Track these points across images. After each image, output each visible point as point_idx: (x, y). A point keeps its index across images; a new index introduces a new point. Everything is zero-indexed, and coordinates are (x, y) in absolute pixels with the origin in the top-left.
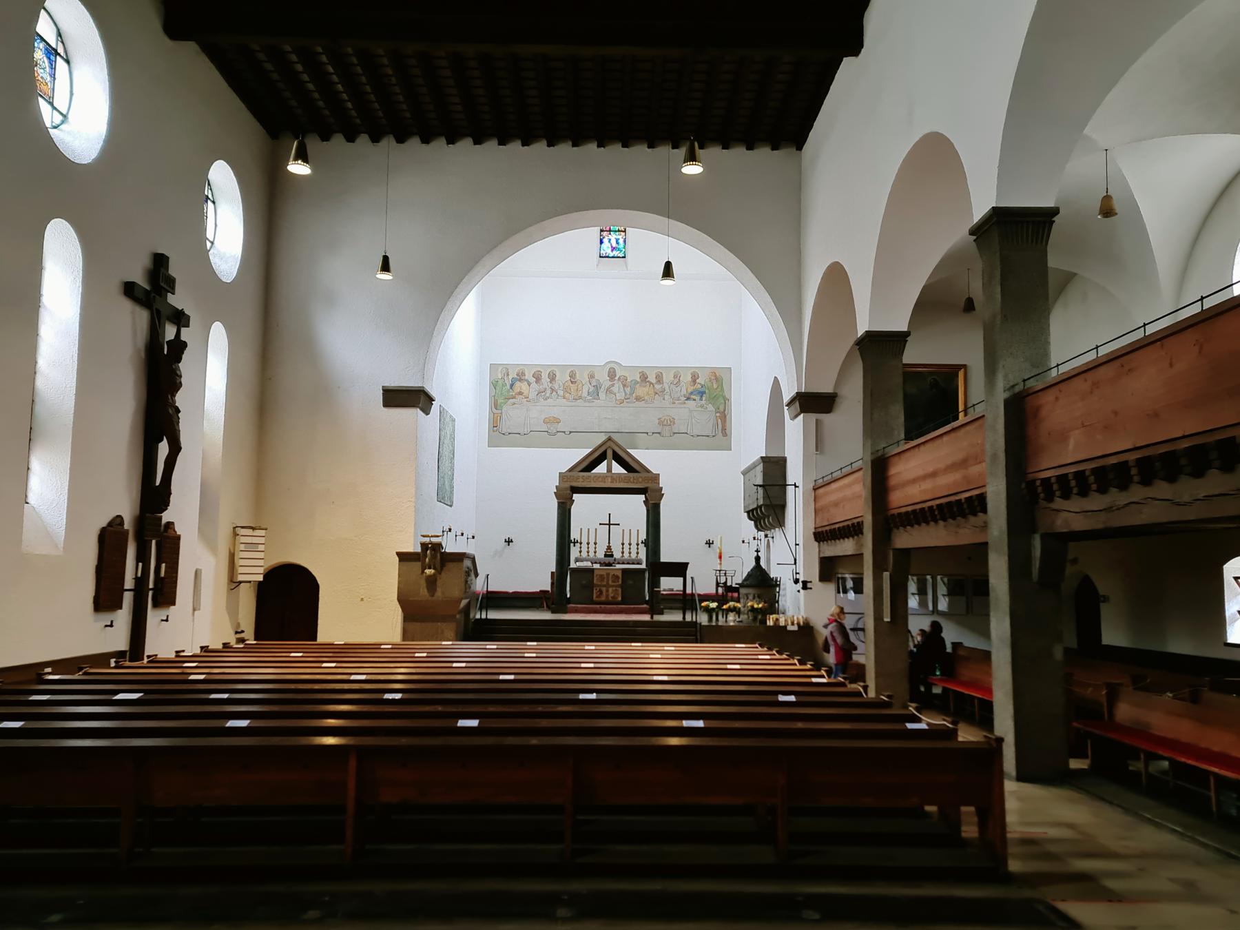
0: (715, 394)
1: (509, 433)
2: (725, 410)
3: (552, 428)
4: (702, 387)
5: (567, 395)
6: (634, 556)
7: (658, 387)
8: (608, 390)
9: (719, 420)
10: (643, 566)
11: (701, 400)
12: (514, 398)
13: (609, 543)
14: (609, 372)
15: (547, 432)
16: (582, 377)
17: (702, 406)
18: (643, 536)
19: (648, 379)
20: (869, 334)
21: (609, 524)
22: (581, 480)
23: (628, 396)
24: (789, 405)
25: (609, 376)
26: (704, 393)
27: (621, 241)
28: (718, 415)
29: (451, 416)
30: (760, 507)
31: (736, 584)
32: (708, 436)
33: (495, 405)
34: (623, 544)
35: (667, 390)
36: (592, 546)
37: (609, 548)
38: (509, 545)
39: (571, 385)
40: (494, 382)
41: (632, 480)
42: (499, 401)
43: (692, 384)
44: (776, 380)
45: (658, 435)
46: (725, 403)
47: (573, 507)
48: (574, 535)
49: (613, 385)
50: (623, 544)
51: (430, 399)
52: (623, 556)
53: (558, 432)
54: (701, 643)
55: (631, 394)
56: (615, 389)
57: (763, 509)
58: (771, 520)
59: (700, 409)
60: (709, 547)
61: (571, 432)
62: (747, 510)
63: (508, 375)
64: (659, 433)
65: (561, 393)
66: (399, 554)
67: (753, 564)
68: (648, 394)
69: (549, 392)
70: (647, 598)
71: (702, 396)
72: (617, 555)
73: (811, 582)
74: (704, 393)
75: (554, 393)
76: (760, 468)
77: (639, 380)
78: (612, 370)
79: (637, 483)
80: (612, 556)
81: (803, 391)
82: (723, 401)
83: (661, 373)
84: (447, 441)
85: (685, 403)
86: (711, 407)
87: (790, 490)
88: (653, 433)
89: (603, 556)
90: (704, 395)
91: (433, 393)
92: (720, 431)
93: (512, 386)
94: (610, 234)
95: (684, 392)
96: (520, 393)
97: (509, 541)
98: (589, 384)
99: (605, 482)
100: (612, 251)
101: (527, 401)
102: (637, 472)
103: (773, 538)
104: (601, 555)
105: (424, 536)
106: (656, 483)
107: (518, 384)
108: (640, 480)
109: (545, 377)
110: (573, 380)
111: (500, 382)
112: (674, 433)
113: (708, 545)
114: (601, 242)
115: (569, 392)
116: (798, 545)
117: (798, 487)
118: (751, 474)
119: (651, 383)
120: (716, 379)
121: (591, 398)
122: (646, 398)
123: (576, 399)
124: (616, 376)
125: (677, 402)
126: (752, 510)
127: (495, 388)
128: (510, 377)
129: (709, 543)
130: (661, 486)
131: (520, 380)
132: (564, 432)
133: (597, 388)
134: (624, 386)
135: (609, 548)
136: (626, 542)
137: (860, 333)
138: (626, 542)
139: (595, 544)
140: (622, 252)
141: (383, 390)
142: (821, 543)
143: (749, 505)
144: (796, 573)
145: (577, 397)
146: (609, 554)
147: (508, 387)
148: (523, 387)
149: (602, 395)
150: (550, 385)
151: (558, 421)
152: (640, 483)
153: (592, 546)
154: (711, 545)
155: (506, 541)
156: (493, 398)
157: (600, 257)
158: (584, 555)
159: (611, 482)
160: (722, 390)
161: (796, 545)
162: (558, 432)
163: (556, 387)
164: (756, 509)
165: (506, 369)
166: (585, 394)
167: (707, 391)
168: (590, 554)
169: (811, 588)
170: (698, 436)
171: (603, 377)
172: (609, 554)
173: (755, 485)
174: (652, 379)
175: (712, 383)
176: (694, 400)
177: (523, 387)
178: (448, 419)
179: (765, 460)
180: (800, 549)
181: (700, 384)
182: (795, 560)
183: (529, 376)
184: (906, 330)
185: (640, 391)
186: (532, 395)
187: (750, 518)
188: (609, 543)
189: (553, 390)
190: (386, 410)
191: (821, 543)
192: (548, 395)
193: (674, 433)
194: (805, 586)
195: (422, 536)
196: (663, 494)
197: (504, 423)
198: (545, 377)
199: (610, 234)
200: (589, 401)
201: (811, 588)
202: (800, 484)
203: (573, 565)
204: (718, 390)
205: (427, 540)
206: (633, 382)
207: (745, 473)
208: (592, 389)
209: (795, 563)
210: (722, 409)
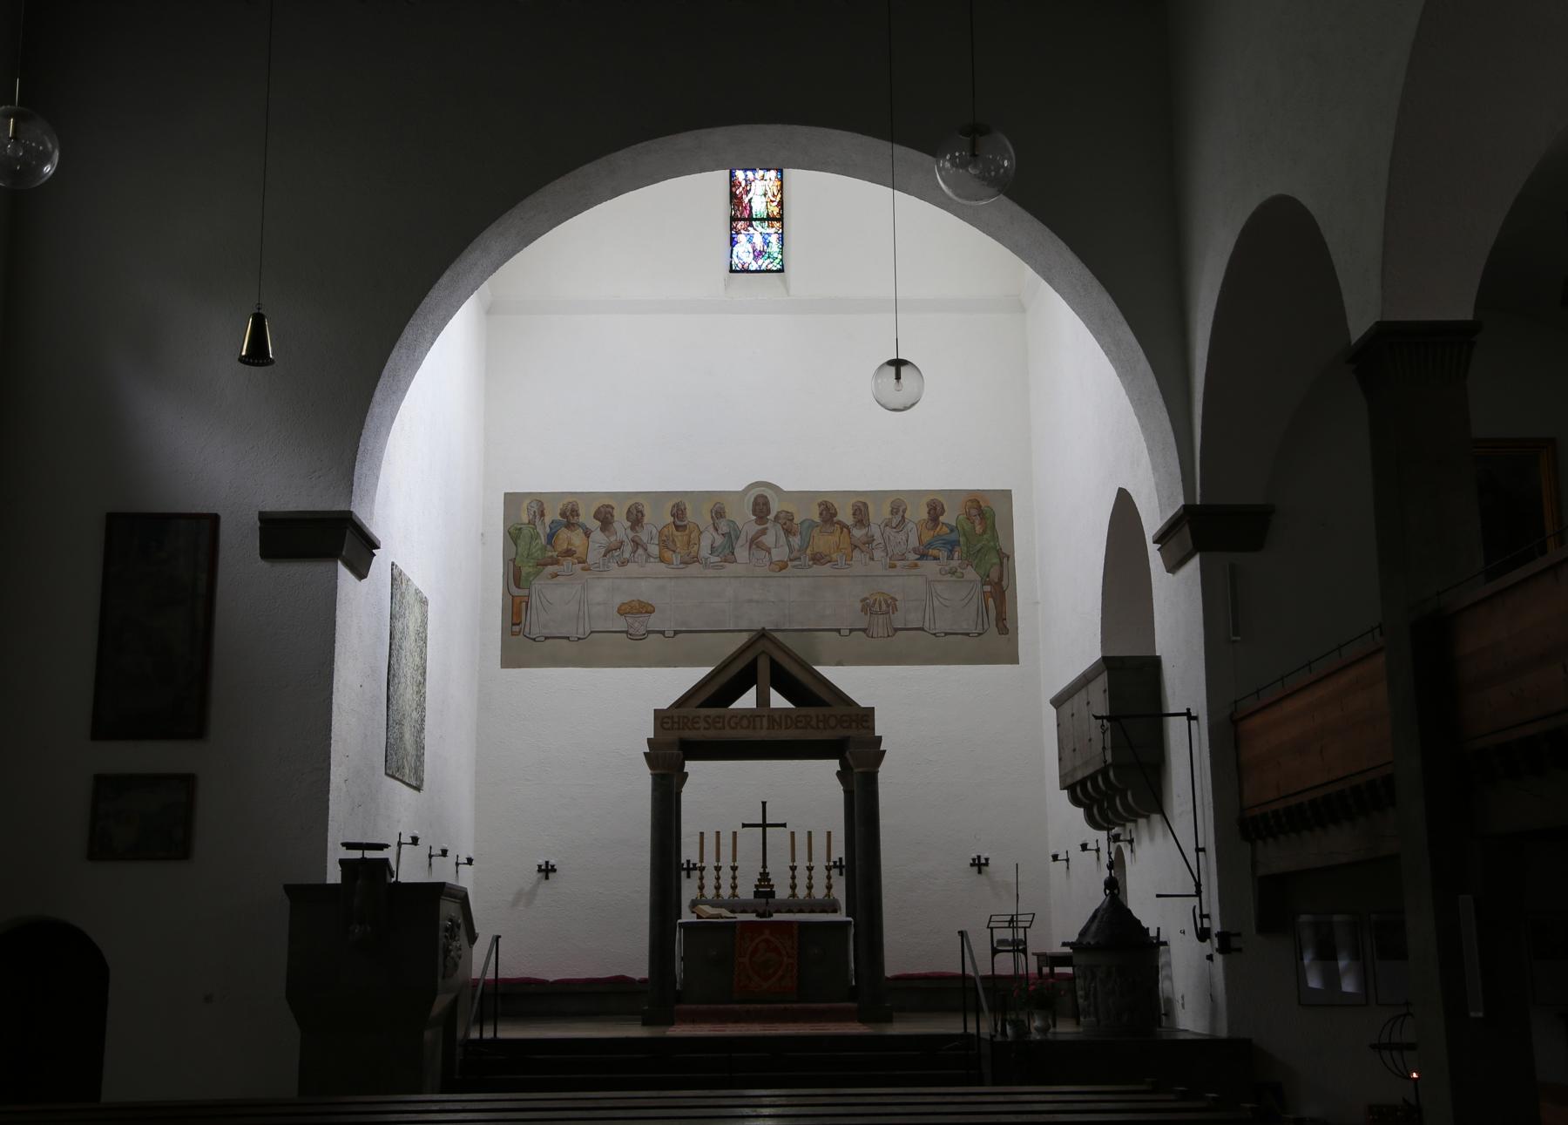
0: (979, 546)
1: (546, 638)
2: (1001, 579)
3: (636, 625)
4: (952, 531)
5: (668, 554)
6: (819, 893)
7: (858, 533)
8: (755, 543)
9: (991, 601)
10: (841, 917)
11: (950, 557)
12: (555, 562)
13: (764, 866)
14: (756, 503)
15: (627, 632)
16: (700, 517)
17: (953, 572)
18: (839, 852)
19: (840, 517)
20: (1384, 333)
21: (764, 825)
23: (795, 554)
24: (1161, 538)
25: (754, 514)
26: (957, 543)
27: (774, 239)
28: (988, 588)
29: (417, 592)
30: (1104, 771)
31: (1064, 944)
32: (968, 634)
33: (516, 577)
34: (793, 868)
35: (878, 539)
36: (726, 874)
37: (764, 876)
38: (547, 878)
39: (676, 533)
40: (512, 530)
41: (814, 723)
42: (525, 570)
43: (930, 525)
44: (1124, 501)
45: (861, 633)
46: (1001, 564)
47: (684, 789)
48: (689, 852)
49: (764, 532)
50: (793, 868)
51: (369, 545)
52: (794, 895)
53: (649, 632)
54: (995, 1084)
55: (803, 549)
56: (769, 539)
57: (1111, 774)
58: (1130, 797)
59: (948, 577)
60: (980, 872)
61: (676, 633)
62: (1069, 781)
63: (542, 514)
64: (864, 630)
65: (654, 549)
66: (290, 890)
67: (1099, 897)
68: (838, 548)
69: (628, 548)
71: (951, 551)
72: (782, 892)
73: (1239, 935)
74: (957, 543)
75: (640, 551)
76: (1102, 681)
77: (817, 519)
78: (761, 501)
79: (825, 729)
80: (772, 894)
81: (1198, 503)
82: (996, 560)
83: (865, 504)
84: (409, 644)
85: (916, 565)
86: (971, 574)
87: (1176, 730)
88: (851, 631)
89: (751, 896)
90: (957, 548)
91: (376, 529)
92: (993, 623)
93: (551, 537)
94: (751, 225)
95: (914, 542)
96: (569, 553)
97: (547, 870)
98: (711, 529)
99: (754, 728)
100: (756, 258)
101: (583, 569)
102: (829, 706)
103: (1131, 841)
104: (746, 891)
105: (349, 846)
106: (868, 728)
107: (564, 534)
108: (832, 722)
109: (621, 523)
110: (679, 523)
111: (525, 532)
112: (896, 630)
113: (976, 868)
114: (733, 242)
115: (674, 549)
116: (1203, 850)
117: (1195, 718)
118: (1079, 700)
119: (843, 526)
120: (981, 513)
121: (717, 559)
122: (834, 556)
123: (686, 563)
124: (769, 512)
125: (899, 564)
126: (1083, 782)
127: (516, 545)
128: (548, 520)
129: (979, 864)
130: (876, 735)
131: (570, 526)
132: (663, 632)
133: (731, 537)
134: (788, 532)
135: (764, 876)
136: (802, 863)
137: (1358, 326)
138: (802, 863)
139: (734, 869)
140: (777, 261)
141: (261, 520)
142: (1260, 843)
143: (1074, 769)
144: (1202, 916)
145: (687, 559)
146: (764, 888)
147: (543, 540)
148: (577, 538)
149: (742, 553)
150: (631, 534)
151: (650, 609)
152: (833, 728)
153: (726, 874)
154: (984, 868)
155: (540, 870)
156: (511, 564)
157: (732, 271)
158: (710, 892)
159: (768, 729)
160: (995, 537)
161: (1198, 850)
162: (649, 632)
163: (644, 536)
164: (1093, 777)
165: (538, 503)
166: (705, 551)
167: (962, 540)
168: (721, 891)
169: (1239, 950)
170: (946, 634)
171: (743, 517)
172: (764, 888)
173: (1097, 718)
174: (845, 516)
175: (973, 523)
176: (936, 558)
177: (577, 538)
178: (410, 598)
179: (1109, 663)
180: (1210, 861)
181: (947, 525)
182: (1198, 885)
183: (586, 517)
184: (1470, 317)
185: (822, 542)
186: (594, 556)
187: (1075, 801)
188: (764, 866)
189: (637, 544)
190: (264, 565)
191: (1260, 843)
192: (627, 555)
193: (896, 630)
194: (1226, 943)
195: (344, 844)
196: (885, 751)
197: (534, 617)
198: (621, 523)
199: (751, 225)
200: (715, 567)
201: (1239, 950)
202: (1200, 707)
203: (687, 917)
204: (985, 536)
205: (357, 854)
206: (806, 525)
207: (1058, 702)
208: (719, 540)
209: (1198, 893)
210: (994, 575)
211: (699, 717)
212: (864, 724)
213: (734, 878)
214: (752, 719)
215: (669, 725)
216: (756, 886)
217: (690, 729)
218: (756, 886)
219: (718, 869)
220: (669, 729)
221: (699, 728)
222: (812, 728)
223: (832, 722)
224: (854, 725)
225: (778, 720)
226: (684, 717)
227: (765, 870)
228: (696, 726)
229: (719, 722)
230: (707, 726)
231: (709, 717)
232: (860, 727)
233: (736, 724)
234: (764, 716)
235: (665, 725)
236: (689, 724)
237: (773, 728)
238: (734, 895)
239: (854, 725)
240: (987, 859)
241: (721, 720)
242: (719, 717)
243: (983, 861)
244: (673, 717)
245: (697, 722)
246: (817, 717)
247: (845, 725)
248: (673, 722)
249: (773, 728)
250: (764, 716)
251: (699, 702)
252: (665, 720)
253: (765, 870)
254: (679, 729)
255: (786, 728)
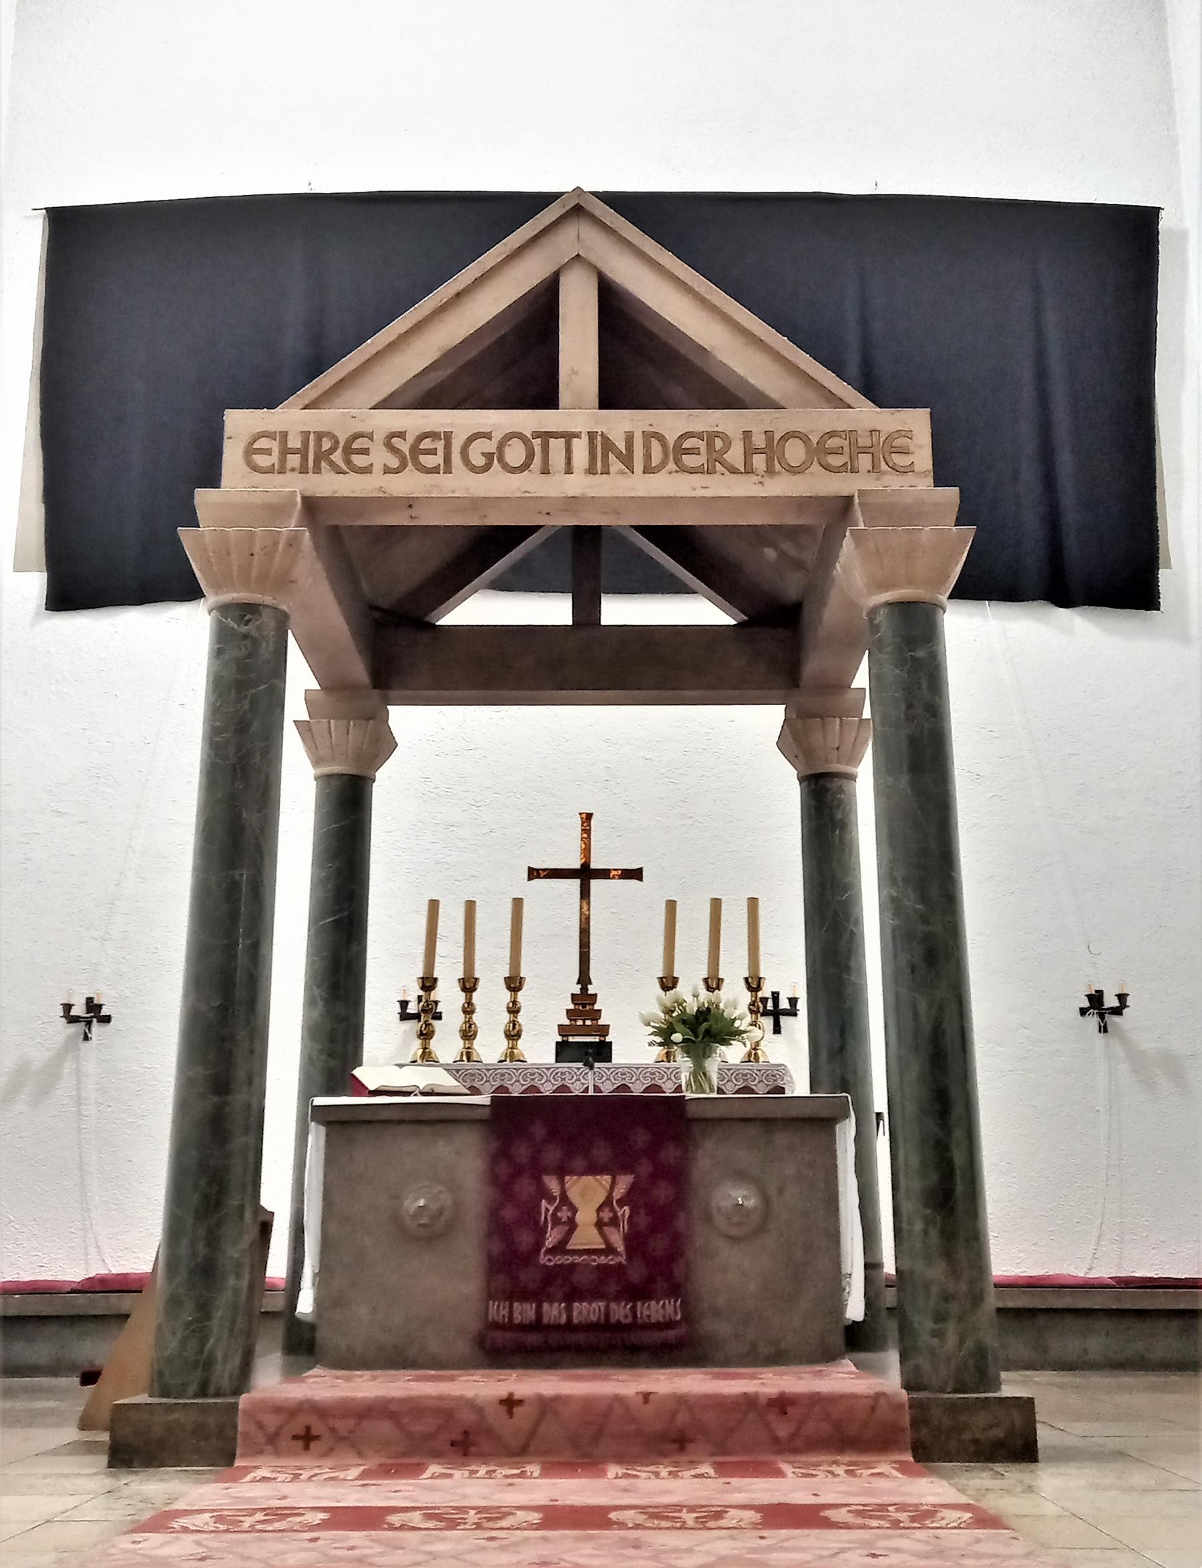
13: (584, 979)
21: (585, 874)
22: (380, 457)
41: (735, 455)
60: (1104, 1029)
70: (855, 1310)
79: (770, 471)
80: (603, 1051)
89: (550, 1058)
152: (792, 470)
159: (591, 471)
168: (477, 1044)
188: (584, 979)
211: (370, 437)
212: (898, 460)
213: (514, 1009)
214: (537, 443)
215: (274, 459)
216: (561, 1028)
217: (340, 472)
218: (561, 1028)
219: (469, 985)
220: (270, 470)
221: (367, 470)
222: (733, 471)
223: (795, 452)
224: (865, 461)
225: (622, 446)
226: (320, 436)
227: (584, 989)
228: (359, 460)
229: (433, 452)
230: (394, 463)
231: (401, 435)
232: (884, 466)
233: (489, 456)
234: (577, 435)
235: (261, 461)
236: (337, 457)
237: (606, 472)
238: (511, 1055)
239: (865, 461)
240: (1122, 997)
241: (440, 445)
242: (434, 435)
243: (1110, 1001)
244: (284, 435)
245: (365, 452)
246: (747, 435)
247: (835, 461)
248: (285, 451)
249: (606, 472)
250: (577, 435)
251: (373, 404)
252: (262, 443)
253: (584, 989)
254: (303, 470)
255: (648, 469)
